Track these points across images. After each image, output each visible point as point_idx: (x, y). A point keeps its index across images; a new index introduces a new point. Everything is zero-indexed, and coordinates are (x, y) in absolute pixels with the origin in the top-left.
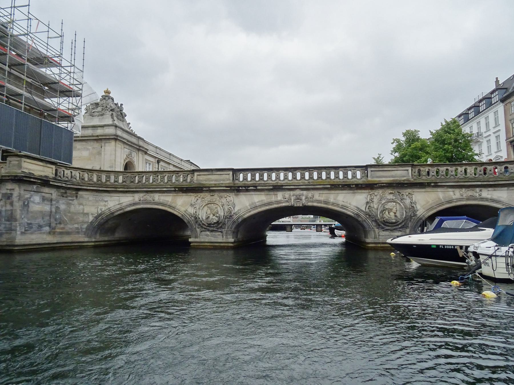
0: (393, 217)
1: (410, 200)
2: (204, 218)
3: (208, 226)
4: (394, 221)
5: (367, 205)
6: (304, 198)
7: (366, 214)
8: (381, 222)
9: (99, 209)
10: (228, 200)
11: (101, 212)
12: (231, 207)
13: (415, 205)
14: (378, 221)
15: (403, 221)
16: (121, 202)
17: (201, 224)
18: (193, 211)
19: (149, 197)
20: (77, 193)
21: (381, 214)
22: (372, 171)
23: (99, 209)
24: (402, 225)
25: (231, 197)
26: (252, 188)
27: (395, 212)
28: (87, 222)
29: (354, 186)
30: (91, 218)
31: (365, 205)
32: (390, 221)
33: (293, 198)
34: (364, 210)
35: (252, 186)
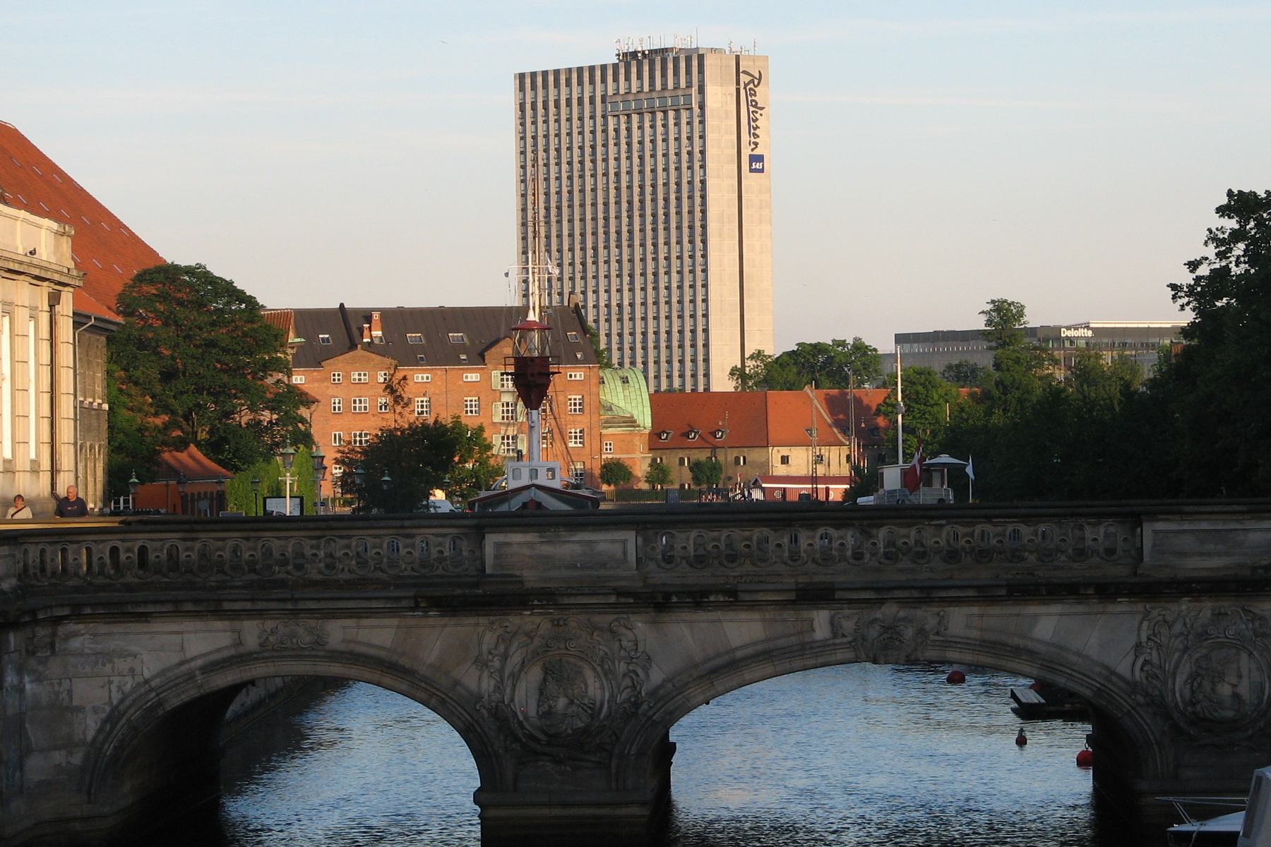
2: (532, 711)
4: (1230, 714)
5: (1137, 657)
6: (909, 633)
7: (1133, 687)
9: (114, 688)
10: (624, 643)
11: (120, 696)
12: (640, 671)
16: (189, 655)
17: (520, 734)
20: (54, 634)
23: (114, 688)
27: (1234, 681)
29: (1091, 591)
30: (90, 726)
31: (1131, 658)
32: (1216, 714)
33: (874, 632)
34: (1127, 675)
35: (718, 592)
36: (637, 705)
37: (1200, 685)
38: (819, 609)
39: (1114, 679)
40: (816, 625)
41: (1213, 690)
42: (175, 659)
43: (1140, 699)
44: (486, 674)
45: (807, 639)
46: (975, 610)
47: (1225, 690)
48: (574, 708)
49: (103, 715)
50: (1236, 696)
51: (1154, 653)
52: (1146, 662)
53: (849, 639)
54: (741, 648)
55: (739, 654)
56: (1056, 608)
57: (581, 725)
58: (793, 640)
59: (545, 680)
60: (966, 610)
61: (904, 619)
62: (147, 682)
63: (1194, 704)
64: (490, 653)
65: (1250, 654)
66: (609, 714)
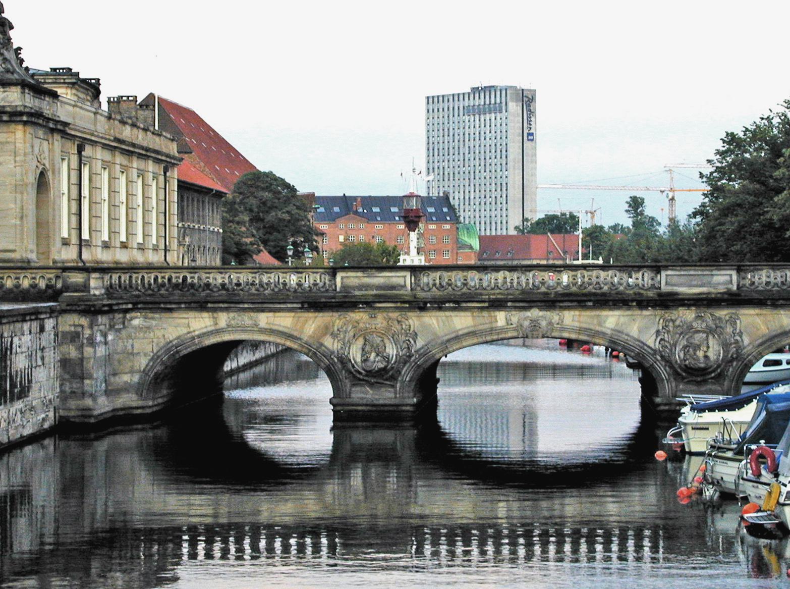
0: (702, 359)
1: (732, 329)
2: (359, 359)
3: (366, 376)
4: (702, 365)
5: (657, 337)
6: (544, 323)
7: (655, 352)
8: (680, 367)
10: (404, 327)
12: (411, 340)
13: (741, 337)
14: (676, 366)
15: (719, 366)
16: (192, 329)
18: (335, 346)
19: (246, 319)
20: (125, 317)
21: (682, 355)
22: (667, 275)
24: (716, 373)
25: (410, 321)
26: (452, 305)
28: (140, 371)
29: (634, 304)
33: (526, 323)
34: (652, 345)
35: (449, 302)
36: (410, 357)
37: (688, 351)
38: (500, 311)
39: (646, 347)
40: (498, 318)
41: (695, 354)
42: (185, 331)
43: (659, 358)
44: (336, 340)
45: (494, 326)
46: (577, 313)
47: (700, 354)
48: (379, 358)
49: (150, 358)
50: (706, 357)
51: (666, 335)
52: (661, 340)
53: (514, 326)
54: (462, 329)
55: (461, 333)
56: (617, 313)
57: (383, 366)
58: (487, 326)
59: (365, 344)
60: (572, 313)
61: (542, 317)
62: (171, 342)
63: (685, 361)
64: (338, 330)
65: (714, 336)
66: (395, 362)
